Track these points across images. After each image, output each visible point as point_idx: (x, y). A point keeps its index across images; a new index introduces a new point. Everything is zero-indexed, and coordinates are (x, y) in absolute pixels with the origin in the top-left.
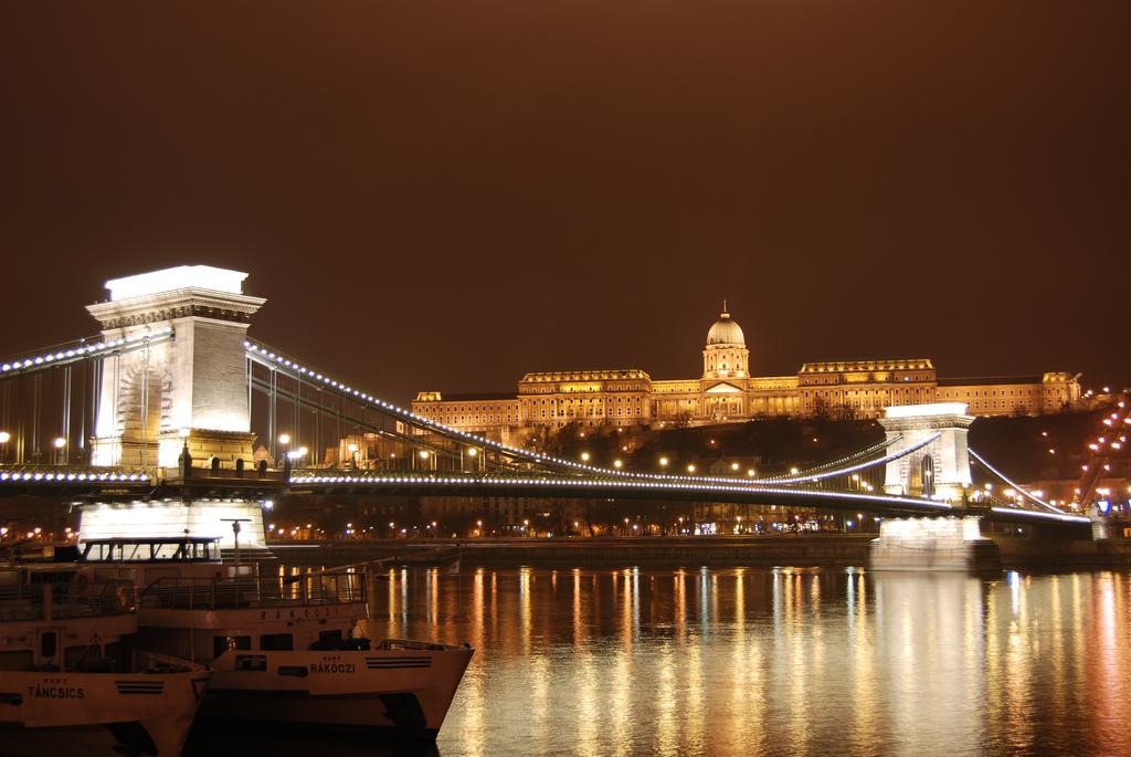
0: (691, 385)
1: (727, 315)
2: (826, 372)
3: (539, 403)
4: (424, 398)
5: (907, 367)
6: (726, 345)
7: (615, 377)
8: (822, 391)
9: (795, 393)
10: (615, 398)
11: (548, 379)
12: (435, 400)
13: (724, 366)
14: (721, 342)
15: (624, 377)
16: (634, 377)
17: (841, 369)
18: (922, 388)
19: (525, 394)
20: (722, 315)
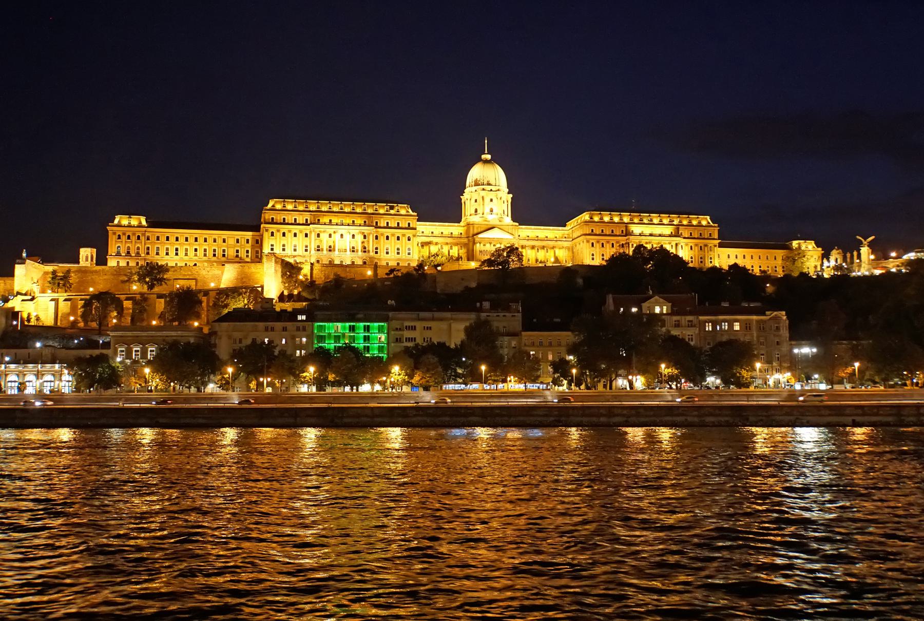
0: (456, 229)
1: (489, 157)
2: (611, 222)
3: (289, 236)
4: (125, 222)
5: (690, 222)
6: (494, 188)
7: (382, 211)
8: (608, 242)
9: (566, 244)
10: (382, 235)
11: (301, 208)
12: (140, 226)
13: (492, 211)
14: (489, 184)
15: (392, 212)
16: (403, 212)
17: (626, 220)
18: (706, 245)
19: (273, 222)
20: (483, 157)
